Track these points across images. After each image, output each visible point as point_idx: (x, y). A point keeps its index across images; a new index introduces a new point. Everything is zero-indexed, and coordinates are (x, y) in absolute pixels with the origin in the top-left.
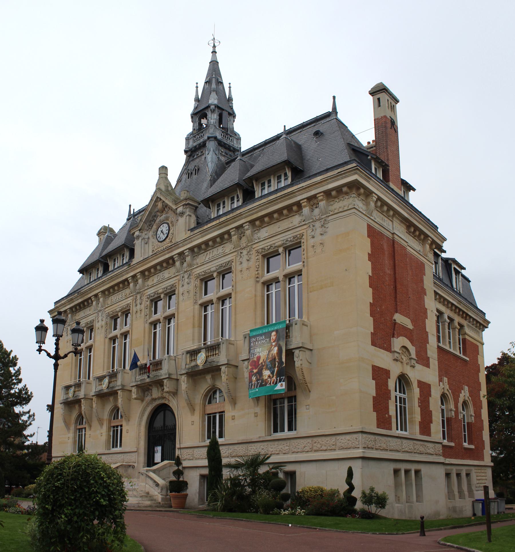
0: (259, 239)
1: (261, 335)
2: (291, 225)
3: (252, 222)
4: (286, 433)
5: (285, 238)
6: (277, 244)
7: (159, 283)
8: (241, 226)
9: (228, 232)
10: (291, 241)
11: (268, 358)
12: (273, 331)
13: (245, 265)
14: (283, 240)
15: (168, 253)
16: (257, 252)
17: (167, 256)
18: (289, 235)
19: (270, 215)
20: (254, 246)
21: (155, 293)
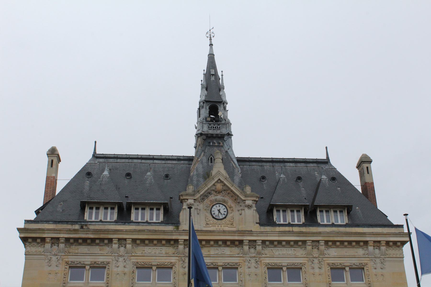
0: (328, 254)
2: (356, 254)
3: (326, 242)
5: (354, 262)
6: (346, 264)
8: (318, 241)
9: (304, 242)
13: (317, 271)
14: (351, 263)
15: (238, 236)
16: (328, 264)
17: (236, 238)
18: (355, 261)
19: (342, 242)
20: (324, 259)
21: (212, 263)
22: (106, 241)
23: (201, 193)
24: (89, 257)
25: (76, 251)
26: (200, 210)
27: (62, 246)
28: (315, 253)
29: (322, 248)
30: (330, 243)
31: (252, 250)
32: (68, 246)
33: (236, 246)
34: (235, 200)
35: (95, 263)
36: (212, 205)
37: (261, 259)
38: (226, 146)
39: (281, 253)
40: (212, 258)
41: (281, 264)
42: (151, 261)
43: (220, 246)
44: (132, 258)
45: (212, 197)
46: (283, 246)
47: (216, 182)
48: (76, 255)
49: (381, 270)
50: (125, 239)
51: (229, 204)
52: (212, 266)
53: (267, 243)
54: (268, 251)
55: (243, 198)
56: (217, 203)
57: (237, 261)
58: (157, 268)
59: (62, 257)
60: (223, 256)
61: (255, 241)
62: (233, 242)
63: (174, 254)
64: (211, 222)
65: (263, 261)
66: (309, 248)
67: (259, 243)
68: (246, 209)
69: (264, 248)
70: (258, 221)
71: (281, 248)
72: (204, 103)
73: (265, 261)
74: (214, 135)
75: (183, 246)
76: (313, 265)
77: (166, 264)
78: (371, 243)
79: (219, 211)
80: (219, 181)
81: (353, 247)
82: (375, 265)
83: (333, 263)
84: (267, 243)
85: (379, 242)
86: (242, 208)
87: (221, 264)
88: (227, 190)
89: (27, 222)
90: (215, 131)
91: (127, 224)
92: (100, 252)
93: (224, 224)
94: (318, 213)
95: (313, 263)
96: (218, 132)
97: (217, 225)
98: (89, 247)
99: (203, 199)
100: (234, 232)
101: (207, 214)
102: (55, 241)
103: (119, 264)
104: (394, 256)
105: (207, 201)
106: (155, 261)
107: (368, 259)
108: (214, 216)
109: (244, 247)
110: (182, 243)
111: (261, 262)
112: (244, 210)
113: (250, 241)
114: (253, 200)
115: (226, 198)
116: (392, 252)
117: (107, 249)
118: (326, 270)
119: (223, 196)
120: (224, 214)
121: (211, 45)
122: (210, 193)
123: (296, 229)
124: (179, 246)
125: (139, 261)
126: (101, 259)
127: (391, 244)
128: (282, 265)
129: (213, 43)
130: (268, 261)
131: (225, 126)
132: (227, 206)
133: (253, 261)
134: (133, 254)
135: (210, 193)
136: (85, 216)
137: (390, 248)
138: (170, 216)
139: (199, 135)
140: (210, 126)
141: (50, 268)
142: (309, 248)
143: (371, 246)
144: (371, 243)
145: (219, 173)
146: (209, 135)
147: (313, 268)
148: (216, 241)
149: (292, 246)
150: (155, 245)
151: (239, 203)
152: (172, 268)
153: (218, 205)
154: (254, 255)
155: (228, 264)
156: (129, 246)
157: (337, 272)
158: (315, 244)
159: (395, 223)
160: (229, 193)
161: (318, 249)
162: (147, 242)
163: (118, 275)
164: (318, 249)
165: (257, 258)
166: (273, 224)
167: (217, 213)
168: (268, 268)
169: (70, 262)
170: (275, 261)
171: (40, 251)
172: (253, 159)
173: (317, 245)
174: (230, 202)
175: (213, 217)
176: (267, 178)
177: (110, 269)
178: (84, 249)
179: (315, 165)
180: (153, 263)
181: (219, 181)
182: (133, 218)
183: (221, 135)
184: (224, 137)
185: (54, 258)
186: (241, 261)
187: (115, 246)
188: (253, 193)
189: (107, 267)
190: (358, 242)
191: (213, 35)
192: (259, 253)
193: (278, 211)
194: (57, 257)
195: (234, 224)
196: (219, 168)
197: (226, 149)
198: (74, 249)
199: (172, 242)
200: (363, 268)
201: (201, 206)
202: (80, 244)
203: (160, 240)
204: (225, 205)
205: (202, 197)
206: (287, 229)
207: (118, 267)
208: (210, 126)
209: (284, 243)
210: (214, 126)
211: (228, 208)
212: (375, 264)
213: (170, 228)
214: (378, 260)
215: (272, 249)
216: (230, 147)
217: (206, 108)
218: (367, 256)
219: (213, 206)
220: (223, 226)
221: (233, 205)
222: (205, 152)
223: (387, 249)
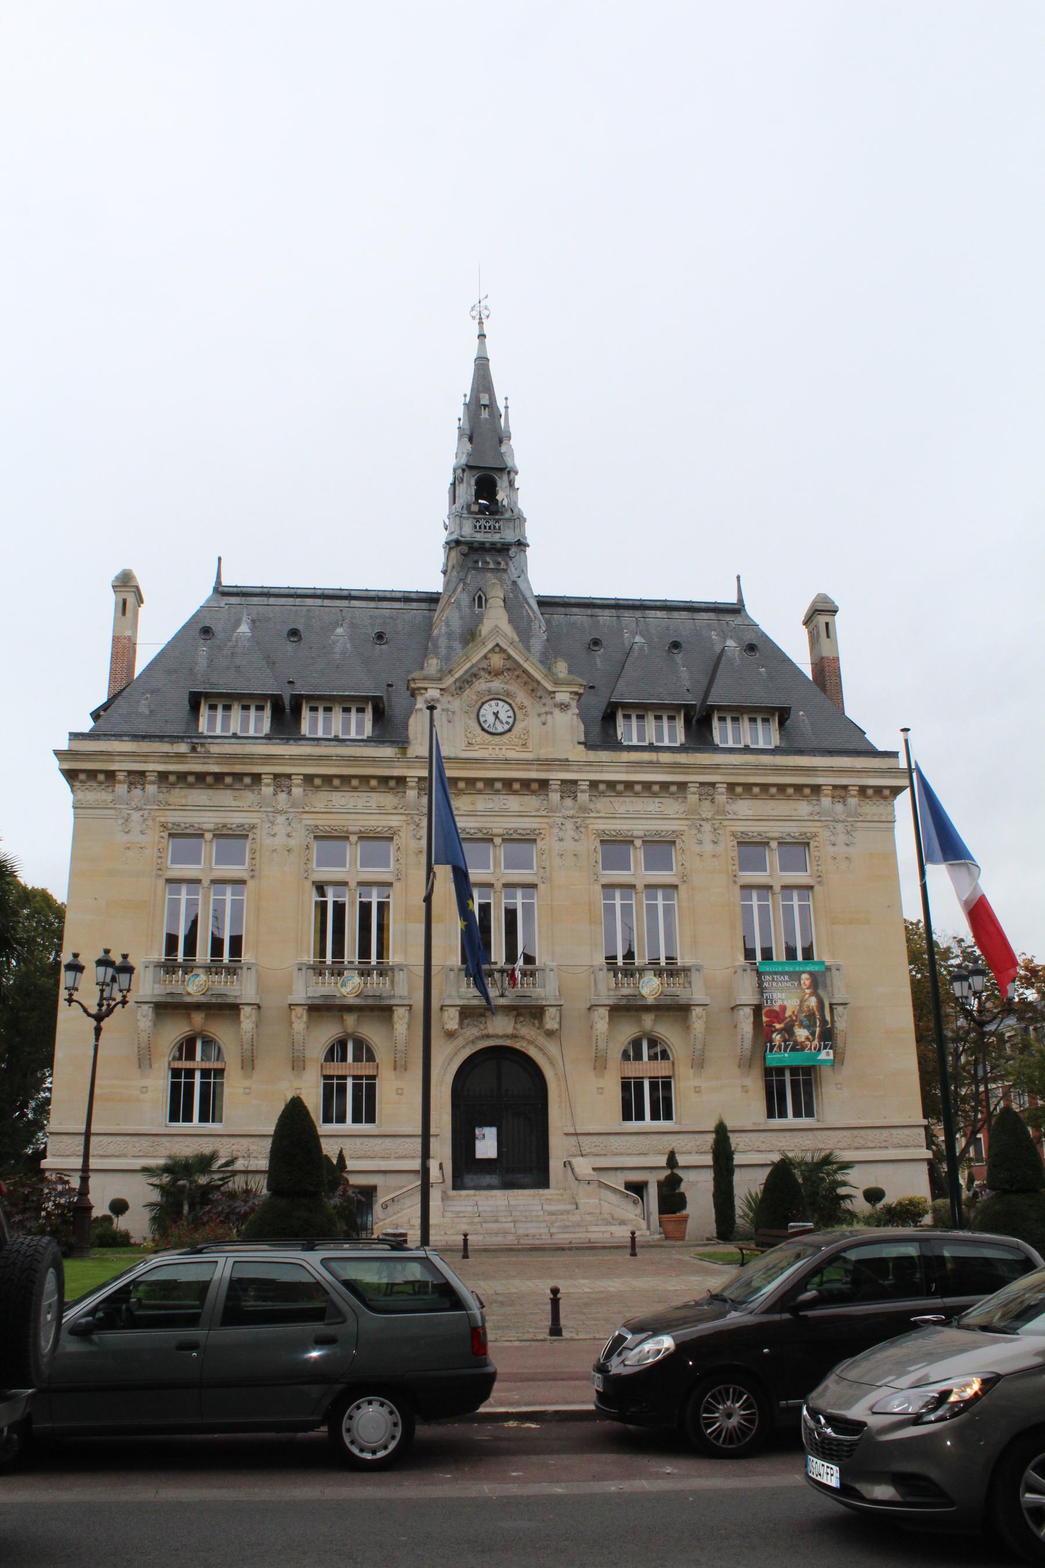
0: (734, 814)
1: (782, 973)
2: (794, 813)
3: (731, 787)
4: (790, 1121)
5: (788, 830)
6: (770, 835)
7: (491, 814)
8: (713, 785)
9: (682, 786)
10: (794, 837)
11: (801, 1010)
12: (804, 972)
13: (708, 847)
15: (537, 770)
16: (733, 834)
17: (534, 775)
18: (792, 829)
19: (765, 787)
20: (726, 823)
21: (480, 830)
22: (247, 780)
23: (457, 676)
24: (210, 814)
25: (183, 802)
26: (454, 712)
27: (151, 789)
28: (706, 809)
29: (721, 798)
30: (739, 790)
31: (568, 802)
32: (165, 790)
33: (533, 792)
34: (533, 690)
35: (225, 826)
36: (480, 703)
37: (588, 821)
38: (513, 569)
39: (631, 809)
40: (479, 819)
41: (630, 833)
42: (346, 823)
43: (497, 792)
44: (305, 816)
45: (481, 685)
46: (637, 795)
47: (489, 651)
48: (183, 808)
49: (845, 847)
50: (289, 776)
51: (518, 700)
52: (480, 835)
53: (602, 787)
54: (603, 804)
55: (551, 689)
56: (491, 697)
57: (535, 826)
58: (359, 838)
59: (153, 813)
60: (503, 813)
61: (575, 782)
62: (526, 783)
63: (396, 808)
64: (478, 739)
65: (591, 827)
66: (693, 798)
67: (584, 786)
68: (557, 712)
69: (594, 798)
70: (582, 739)
71: (632, 799)
72: (463, 471)
73: (596, 827)
74: (487, 545)
75: (416, 792)
76: (699, 836)
77: (379, 829)
78: (827, 791)
79: (496, 714)
80: (497, 649)
81: (789, 798)
82: (832, 838)
83: (742, 833)
84: (602, 787)
85: (845, 787)
86: (547, 709)
87: (500, 831)
88: (513, 669)
89: (75, 736)
90: (489, 535)
91: (292, 742)
92: (234, 803)
93: (506, 744)
94: (716, 723)
95: (699, 831)
96: (496, 538)
97: (491, 747)
98: (210, 792)
99: (461, 688)
100: (528, 762)
101: (469, 722)
102: (137, 777)
103: (276, 829)
104: (876, 818)
105: (469, 694)
106: (356, 824)
107: (819, 824)
108: (486, 726)
109: (550, 794)
110: (414, 784)
111: (586, 827)
112: (551, 713)
113: (564, 782)
114: (571, 693)
115: (513, 688)
116: (872, 809)
117: (249, 798)
118: (728, 847)
119: (506, 683)
120: (507, 723)
121: (482, 336)
122: (475, 675)
123: (665, 757)
124: (408, 791)
125: (320, 823)
126: (236, 819)
127: (870, 792)
128: (632, 836)
129: (486, 332)
130: (602, 827)
131: (511, 525)
132: (513, 705)
133: (569, 825)
134: (307, 809)
135: (475, 675)
136: (201, 724)
137: (867, 801)
138: (387, 724)
139: (453, 545)
140: (478, 525)
141: (127, 838)
142: (693, 798)
143: (826, 796)
144: (827, 791)
145: (496, 630)
146: (476, 545)
147: (700, 842)
148: (489, 782)
149: (655, 795)
150: (355, 789)
151: (540, 697)
152: (392, 838)
153: (493, 703)
154: (571, 813)
155: (515, 831)
156: (297, 791)
157: (750, 848)
158: (706, 789)
159: (880, 749)
160: (518, 677)
161: (713, 801)
162: (336, 782)
163: (275, 855)
164: (713, 801)
165: (579, 820)
166: (615, 746)
167: (491, 719)
168: (601, 841)
169: (170, 825)
170: (618, 827)
171: (105, 801)
172: (573, 601)
173: (711, 792)
174: (521, 697)
175: (483, 729)
176: (604, 643)
177: (258, 841)
178: (199, 796)
179: (712, 615)
180: (351, 829)
181: (497, 649)
182: (305, 729)
183: (503, 544)
184: (508, 550)
185: (136, 816)
186: (544, 826)
187: (267, 790)
188: (571, 677)
189: (251, 836)
190: (798, 788)
191: (486, 313)
192: (584, 809)
193: (627, 717)
194: (141, 813)
195: (530, 745)
196: (496, 620)
197: (514, 578)
198: (179, 795)
199: (392, 783)
200: (808, 844)
201: (456, 704)
202: (191, 786)
203: (365, 779)
204: (510, 701)
205: (458, 684)
206: (646, 756)
207: (274, 835)
208: (478, 525)
209: (638, 788)
210: (488, 525)
211: (516, 709)
212: (833, 834)
213: (388, 752)
214: (840, 827)
215: (612, 799)
216: (523, 572)
217: (469, 484)
218: (816, 818)
219: (483, 704)
220: (504, 748)
221: (526, 703)
222: (465, 584)
223: (862, 803)
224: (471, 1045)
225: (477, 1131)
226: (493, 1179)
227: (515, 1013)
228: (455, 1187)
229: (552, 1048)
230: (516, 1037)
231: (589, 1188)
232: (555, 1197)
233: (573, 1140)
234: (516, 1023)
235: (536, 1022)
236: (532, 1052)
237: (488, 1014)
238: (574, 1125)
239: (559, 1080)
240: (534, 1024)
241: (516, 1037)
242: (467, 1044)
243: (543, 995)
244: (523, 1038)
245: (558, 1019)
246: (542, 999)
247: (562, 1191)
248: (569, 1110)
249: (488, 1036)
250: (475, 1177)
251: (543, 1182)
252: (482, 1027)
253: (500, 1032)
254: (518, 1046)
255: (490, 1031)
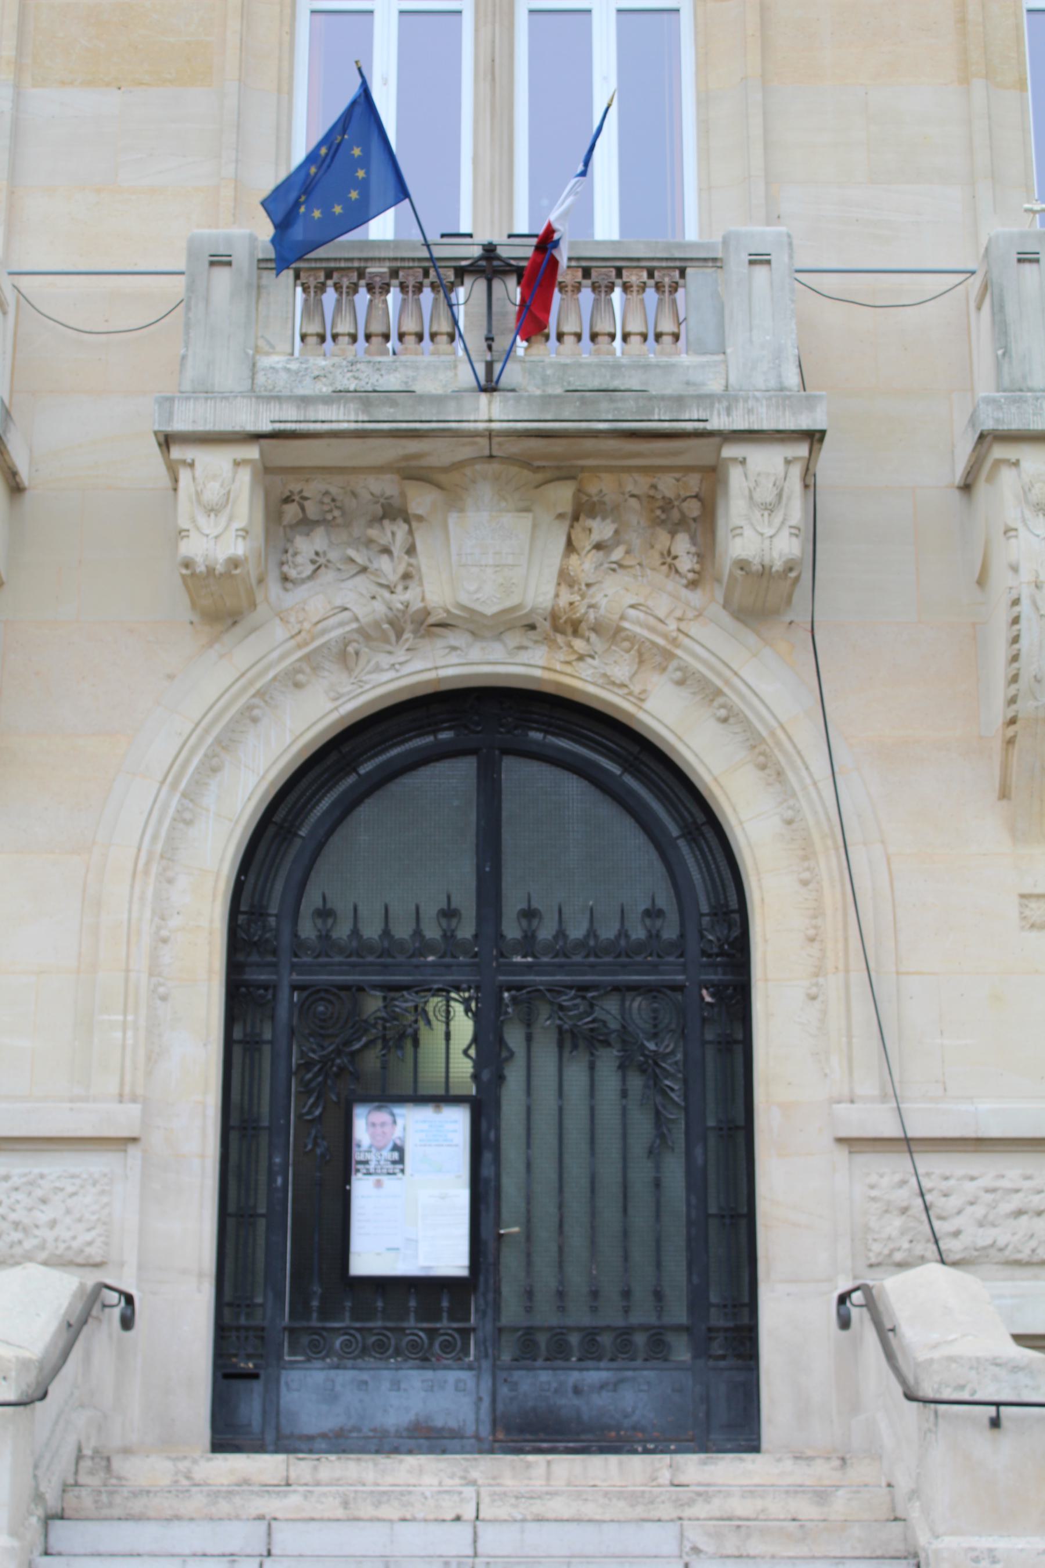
224: (334, 677)
225: (367, 1127)
226: (446, 1392)
227: (563, 495)
228: (228, 1435)
229: (767, 679)
230: (575, 628)
231: (998, 1454)
232: (776, 1507)
233: (889, 1172)
234: (570, 546)
235: (682, 545)
236: (664, 713)
237: (421, 500)
238: (892, 1094)
239: (807, 854)
240: (669, 559)
241: (575, 628)
242: (312, 662)
243: (715, 386)
244: (613, 633)
245: (796, 511)
246: (707, 399)
247: (822, 1472)
248: (862, 1010)
249: (430, 626)
250: (344, 1377)
251: (731, 1419)
252: (388, 568)
253: (487, 595)
254: (589, 676)
255: (436, 591)
